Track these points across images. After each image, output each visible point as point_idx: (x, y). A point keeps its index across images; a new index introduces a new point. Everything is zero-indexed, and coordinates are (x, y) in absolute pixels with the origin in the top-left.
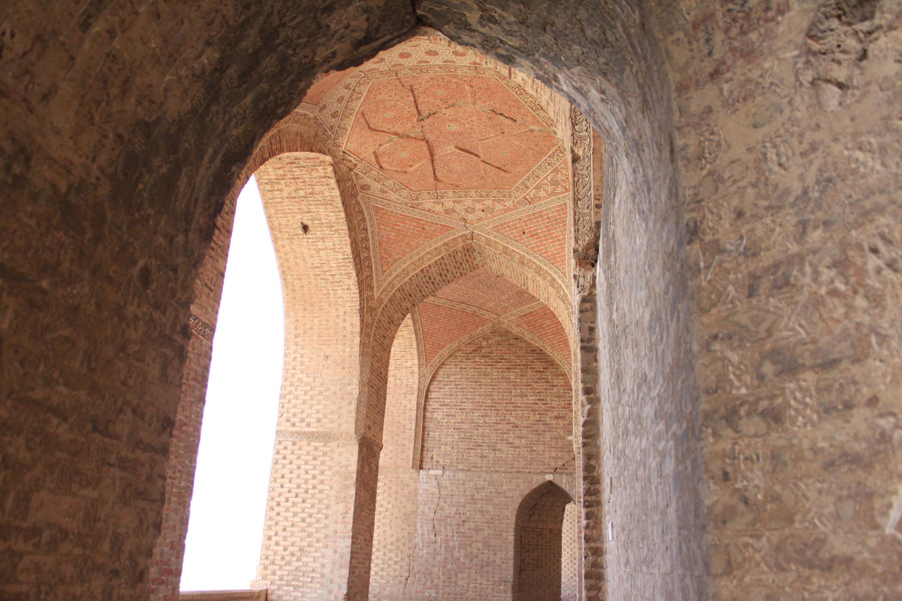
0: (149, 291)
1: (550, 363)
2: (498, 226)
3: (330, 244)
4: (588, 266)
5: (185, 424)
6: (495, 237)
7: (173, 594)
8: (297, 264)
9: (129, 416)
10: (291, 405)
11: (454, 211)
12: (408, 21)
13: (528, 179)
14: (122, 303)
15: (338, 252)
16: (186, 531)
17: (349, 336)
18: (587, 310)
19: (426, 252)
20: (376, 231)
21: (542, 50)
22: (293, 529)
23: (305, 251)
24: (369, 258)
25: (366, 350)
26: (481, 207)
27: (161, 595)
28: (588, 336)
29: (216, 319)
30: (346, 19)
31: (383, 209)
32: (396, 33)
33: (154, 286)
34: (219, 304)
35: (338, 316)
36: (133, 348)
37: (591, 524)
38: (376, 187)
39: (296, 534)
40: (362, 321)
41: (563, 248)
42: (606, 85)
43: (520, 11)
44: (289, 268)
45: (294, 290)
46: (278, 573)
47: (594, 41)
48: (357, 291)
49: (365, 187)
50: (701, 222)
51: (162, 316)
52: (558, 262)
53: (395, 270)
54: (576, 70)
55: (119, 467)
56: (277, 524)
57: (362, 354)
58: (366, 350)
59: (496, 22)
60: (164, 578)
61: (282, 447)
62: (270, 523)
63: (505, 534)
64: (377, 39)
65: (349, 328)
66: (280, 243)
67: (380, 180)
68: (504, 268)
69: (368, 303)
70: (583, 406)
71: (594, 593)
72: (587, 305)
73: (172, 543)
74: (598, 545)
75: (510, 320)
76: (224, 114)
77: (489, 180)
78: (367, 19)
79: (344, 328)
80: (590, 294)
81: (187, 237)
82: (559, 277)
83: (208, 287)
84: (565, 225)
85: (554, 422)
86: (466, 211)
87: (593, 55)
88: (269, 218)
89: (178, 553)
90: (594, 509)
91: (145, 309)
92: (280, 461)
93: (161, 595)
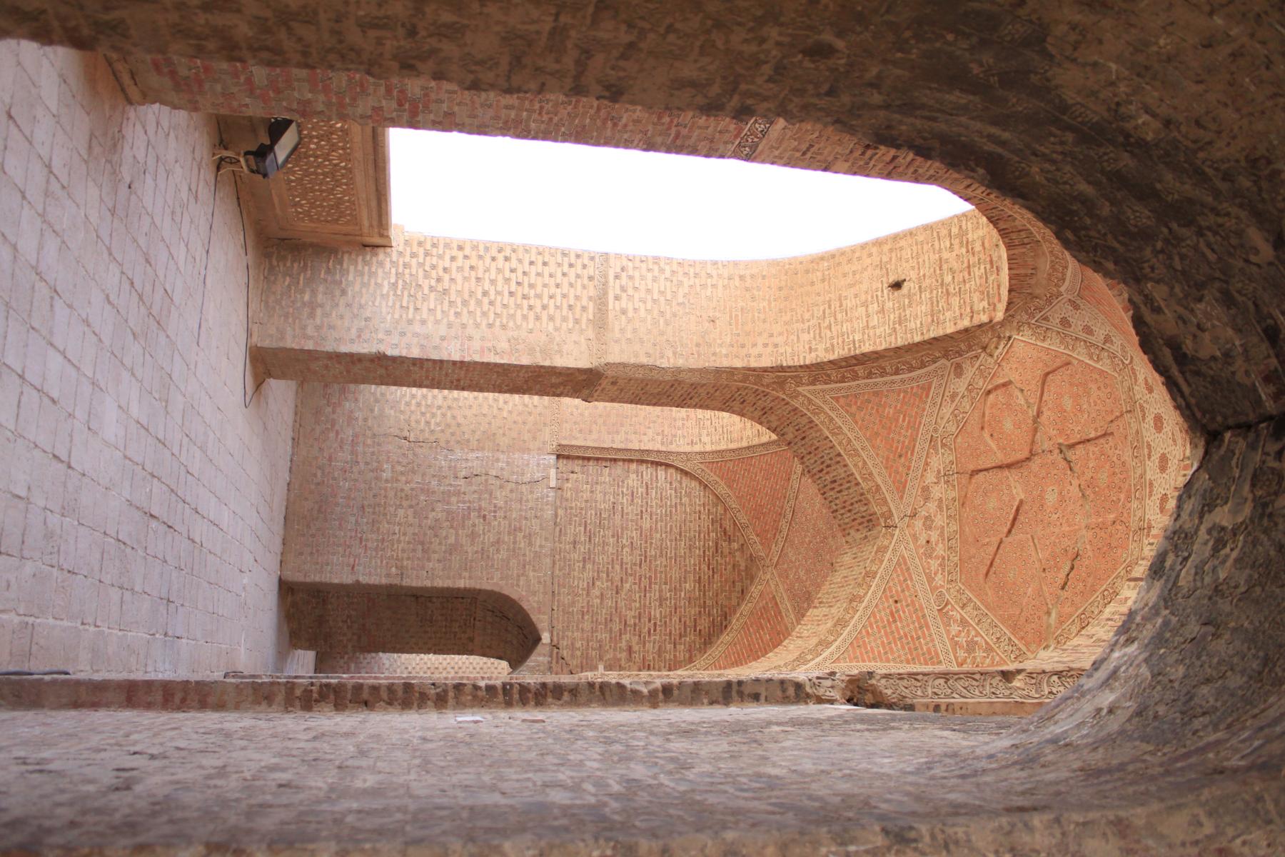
0: (800, 56)
1: (708, 640)
2: (905, 563)
3: (874, 321)
4: (849, 694)
5: (615, 125)
6: (890, 560)
7: (386, 119)
8: (845, 275)
9: (625, 38)
10: (644, 272)
11: (927, 499)
12: (1213, 419)
13: (976, 608)
14: (782, 19)
15: (863, 334)
16: (470, 133)
17: (744, 351)
18: (784, 691)
19: (866, 460)
20: (896, 387)
21: (1174, 619)
22: (473, 280)
23: (864, 287)
24: (856, 378)
25: (724, 376)
26: (933, 540)
27: (384, 103)
28: (746, 692)
29: (763, 162)
30: (1214, 326)
31: (927, 396)
32: (1193, 401)
33: (807, 64)
34: (785, 165)
35: (771, 335)
36: (718, 39)
37: (480, 693)
38: (960, 386)
39: (466, 284)
40: (765, 370)
41: (874, 659)
42: (1122, 716)
43: (1236, 587)
44: (839, 264)
45: (807, 272)
46: (414, 261)
47: (1191, 699)
48: (808, 362)
49: (959, 370)
50: (916, 849)
51: (766, 77)
52: (854, 652)
53: (839, 416)
54: (1144, 670)
55: (554, 28)
56: (480, 257)
57: (718, 371)
58: (724, 376)
59: (1216, 550)
60: (407, 106)
61: (586, 262)
62: (481, 248)
63: (466, 574)
64: (1182, 373)
65: (754, 351)
66: (874, 250)
67: (970, 391)
68: (845, 573)
69: (792, 377)
70: (646, 683)
71: (384, 695)
72: (791, 691)
73: (453, 114)
74: (451, 701)
75: (768, 583)
76: (1062, 153)
77: (973, 551)
78: (1214, 358)
79: (754, 345)
80: (808, 696)
81: (880, 107)
82: (832, 654)
83: (808, 149)
84: (908, 662)
85: (624, 644)
86: (927, 518)
87: (1169, 696)
88: (911, 233)
89: (440, 123)
90: (501, 697)
91: (774, 53)
92: (566, 259)
93: (384, 103)
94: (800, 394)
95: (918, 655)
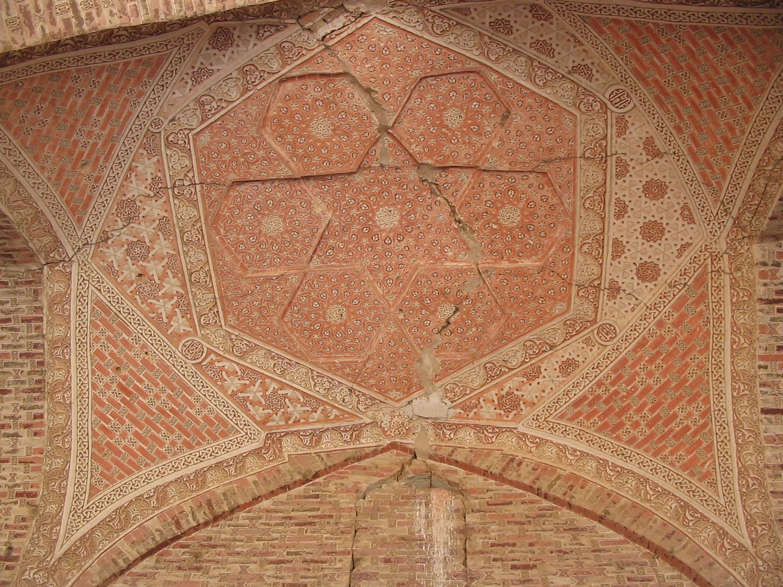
6: (79, 313)
86: (131, 244)
95: (197, 432)
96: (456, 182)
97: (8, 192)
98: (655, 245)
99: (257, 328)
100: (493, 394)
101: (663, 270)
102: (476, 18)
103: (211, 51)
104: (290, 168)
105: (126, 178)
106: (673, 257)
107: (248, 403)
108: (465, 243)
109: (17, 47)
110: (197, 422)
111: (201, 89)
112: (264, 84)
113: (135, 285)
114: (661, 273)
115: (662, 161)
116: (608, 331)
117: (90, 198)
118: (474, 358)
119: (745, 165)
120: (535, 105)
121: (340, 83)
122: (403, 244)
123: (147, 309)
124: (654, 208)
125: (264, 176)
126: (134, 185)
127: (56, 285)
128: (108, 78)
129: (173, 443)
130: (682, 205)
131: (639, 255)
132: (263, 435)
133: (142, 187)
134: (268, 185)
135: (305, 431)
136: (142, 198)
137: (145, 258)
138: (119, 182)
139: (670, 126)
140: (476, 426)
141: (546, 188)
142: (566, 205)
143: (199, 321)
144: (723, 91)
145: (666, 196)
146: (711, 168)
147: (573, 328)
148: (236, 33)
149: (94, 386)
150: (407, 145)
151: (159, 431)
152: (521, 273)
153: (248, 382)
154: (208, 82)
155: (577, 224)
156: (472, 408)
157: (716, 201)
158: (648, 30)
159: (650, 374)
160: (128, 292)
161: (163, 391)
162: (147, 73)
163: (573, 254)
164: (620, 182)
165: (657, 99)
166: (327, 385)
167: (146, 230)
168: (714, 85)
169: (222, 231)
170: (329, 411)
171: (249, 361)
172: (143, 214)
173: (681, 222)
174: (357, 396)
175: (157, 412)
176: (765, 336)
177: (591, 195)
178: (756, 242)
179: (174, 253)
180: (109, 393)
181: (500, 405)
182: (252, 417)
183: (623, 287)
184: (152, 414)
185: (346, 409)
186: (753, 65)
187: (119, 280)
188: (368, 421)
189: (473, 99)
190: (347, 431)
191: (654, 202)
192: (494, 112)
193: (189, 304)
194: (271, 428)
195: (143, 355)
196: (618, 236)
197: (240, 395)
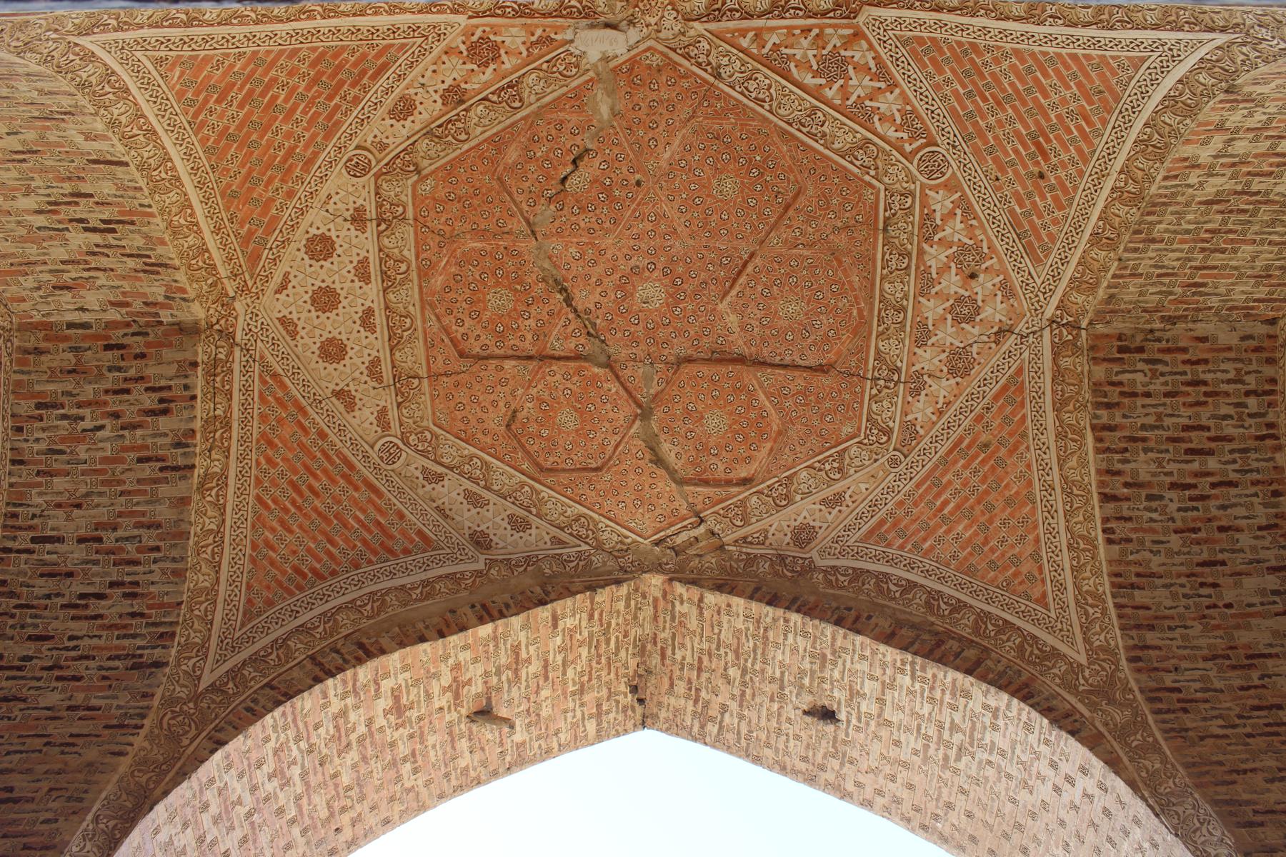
6: (1065, 261)
20: (928, 563)
24: (984, 617)
31: (882, 522)
38: (805, 510)
49: (803, 536)
53: (1058, 568)
67: (787, 496)
77: (841, 240)
86: (970, 320)
94: (1092, 651)
95: (959, 60)
96: (566, 338)
97: (1075, 458)
98: (318, 283)
99: (836, 180)
100: (508, 63)
101: (302, 254)
102: (544, 534)
103: (817, 524)
104: (757, 379)
105: (948, 404)
106: (293, 272)
107: (874, 70)
108: (555, 265)
109: (971, 679)
110: (953, 71)
111: (838, 487)
112: (769, 483)
113: (984, 266)
114: (303, 250)
115: (332, 386)
116: (357, 169)
117: (996, 398)
118: (537, 114)
119: (244, 423)
120: (479, 436)
121: (690, 472)
122: (633, 262)
123: (978, 232)
124: (330, 328)
125: (789, 374)
126: (943, 393)
127: (1080, 300)
128: (925, 540)
129: (997, 61)
130: (298, 337)
131: (335, 268)
132: (861, 19)
133: (935, 387)
134: (788, 360)
135: (796, 17)
136: (938, 374)
137: (959, 300)
138: (957, 405)
139: (332, 437)
140: (531, 16)
141: (459, 337)
142: (433, 318)
143: (913, 202)
144: (289, 506)
145: (318, 345)
146: (278, 400)
147: (405, 164)
148: (787, 539)
149: (1081, 174)
150: (622, 392)
151: (1012, 85)
152: (481, 234)
153: (868, 103)
154: (828, 492)
155: (417, 296)
156: (537, 42)
157: (262, 357)
158: (375, 553)
159: (289, 135)
160: (995, 260)
161: (990, 128)
162: (886, 527)
163: (417, 257)
164: (374, 353)
165: (352, 467)
166: (752, 85)
167: (947, 335)
168: (299, 508)
169: (855, 312)
170: (754, 45)
171: (858, 136)
172: (943, 356)
173: (295, 316)
174: (710, 63)
175: (1007, 107)
176: (159, 235)
177: (405, 334)
178: (203, 323)
179: (921, 299)
180: (1065, 157)
181: (495, 48)
182: (871, 47)
183: (348, 225)
184: (1014, 108)
185: (729, 48)
186: (271, 553)
187: (1001, 277)
188: (696, 24)
189: (548, 439)
190: (731, 10)
191: (330, 336)
192: (524, 425)
193: (921, 228)
194: (847, 26)
195: (1003, 179)
196: (365, 287)
197: (883, 85)
